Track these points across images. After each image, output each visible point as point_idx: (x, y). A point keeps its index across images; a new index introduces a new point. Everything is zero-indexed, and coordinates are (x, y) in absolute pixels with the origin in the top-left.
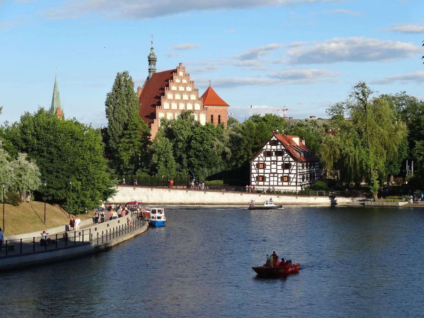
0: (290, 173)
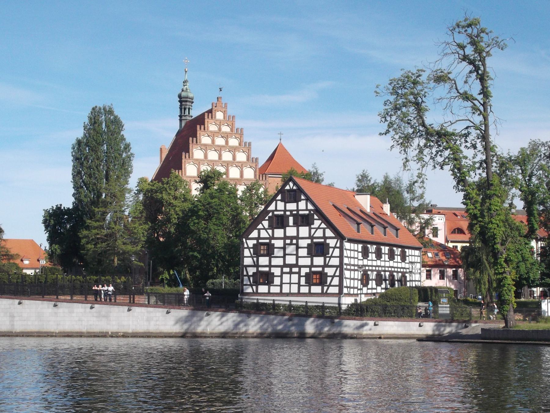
0: (326, 265)
